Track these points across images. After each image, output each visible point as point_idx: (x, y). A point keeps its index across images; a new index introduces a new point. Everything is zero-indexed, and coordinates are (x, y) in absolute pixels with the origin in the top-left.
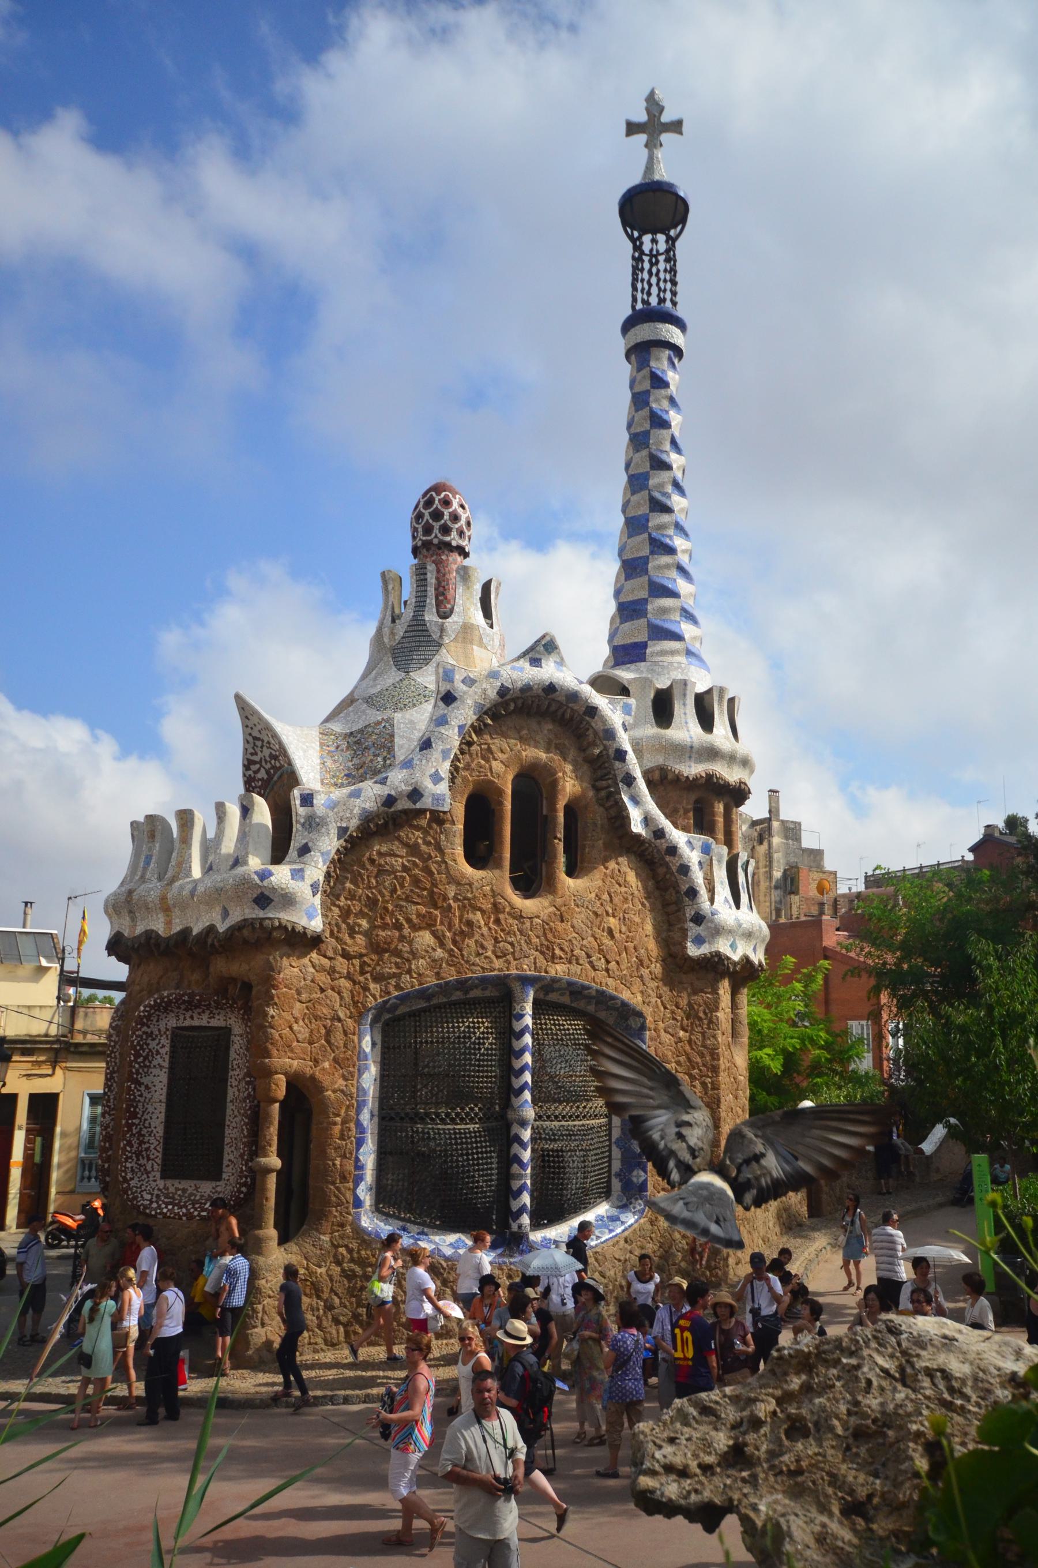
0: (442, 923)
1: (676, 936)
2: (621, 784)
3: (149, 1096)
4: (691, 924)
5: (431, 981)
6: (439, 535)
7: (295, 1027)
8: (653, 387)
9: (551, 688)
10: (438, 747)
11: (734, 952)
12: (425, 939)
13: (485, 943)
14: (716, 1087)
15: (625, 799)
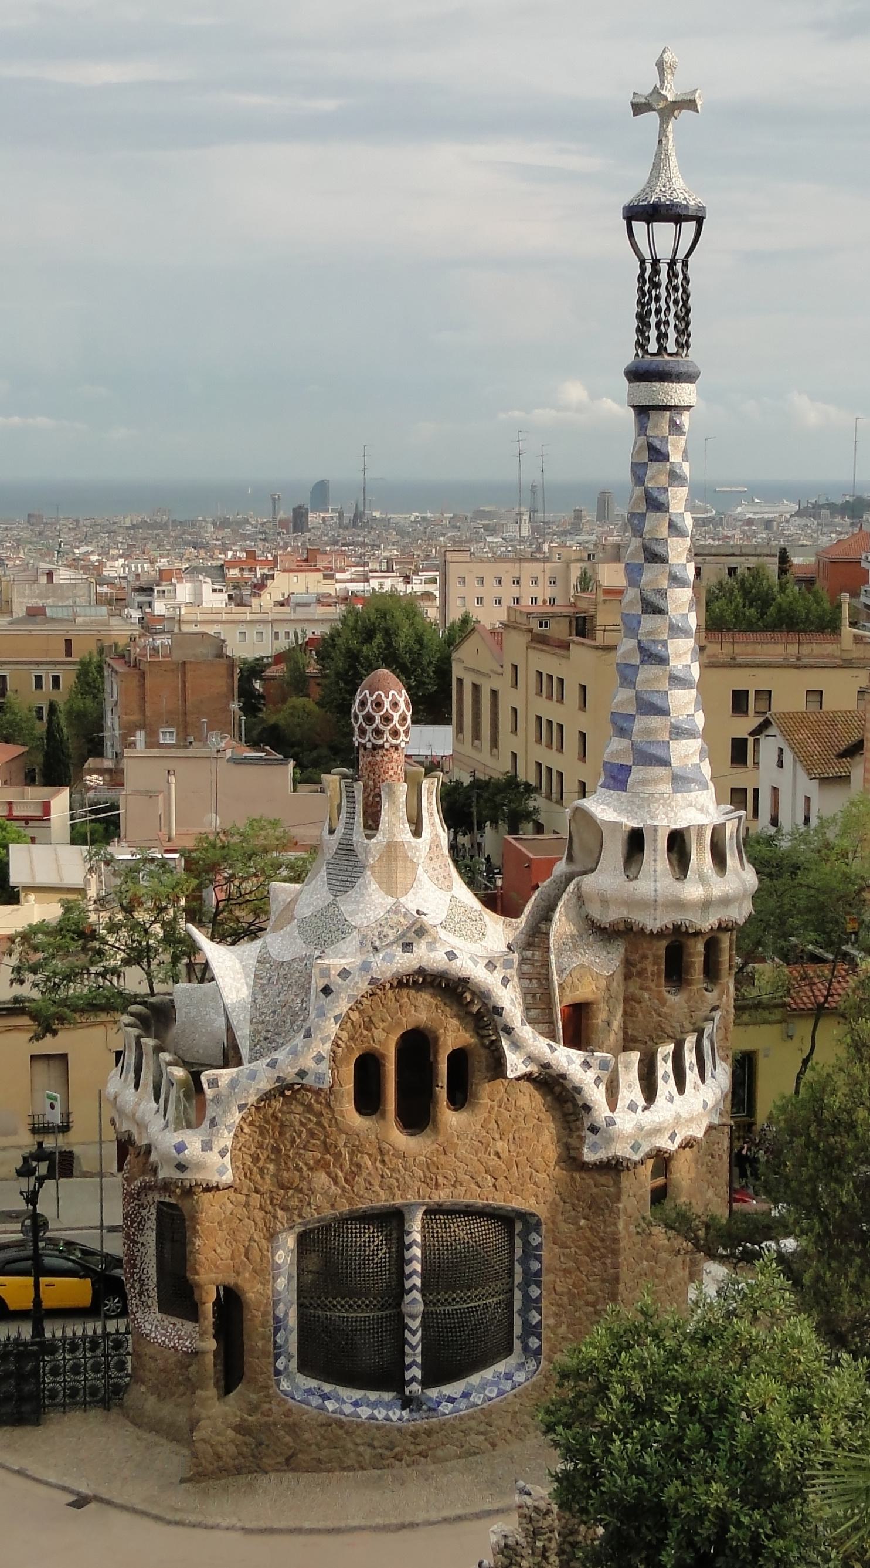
0: (334, 1166)
1: (574, 1142)
2: (501, 1033)
3: (145, 1251)
4: (589, 1133)
5: (328, 1212)
6: (372, 739)
7: (219, 1250)
8: (651, 460)
9: (421, 971)
10: (317, 1035)
11: (636, 1153)
12: (321, 1179)
13: (372, 1181)
14: (616, 1266)
15: (505, 1045)
